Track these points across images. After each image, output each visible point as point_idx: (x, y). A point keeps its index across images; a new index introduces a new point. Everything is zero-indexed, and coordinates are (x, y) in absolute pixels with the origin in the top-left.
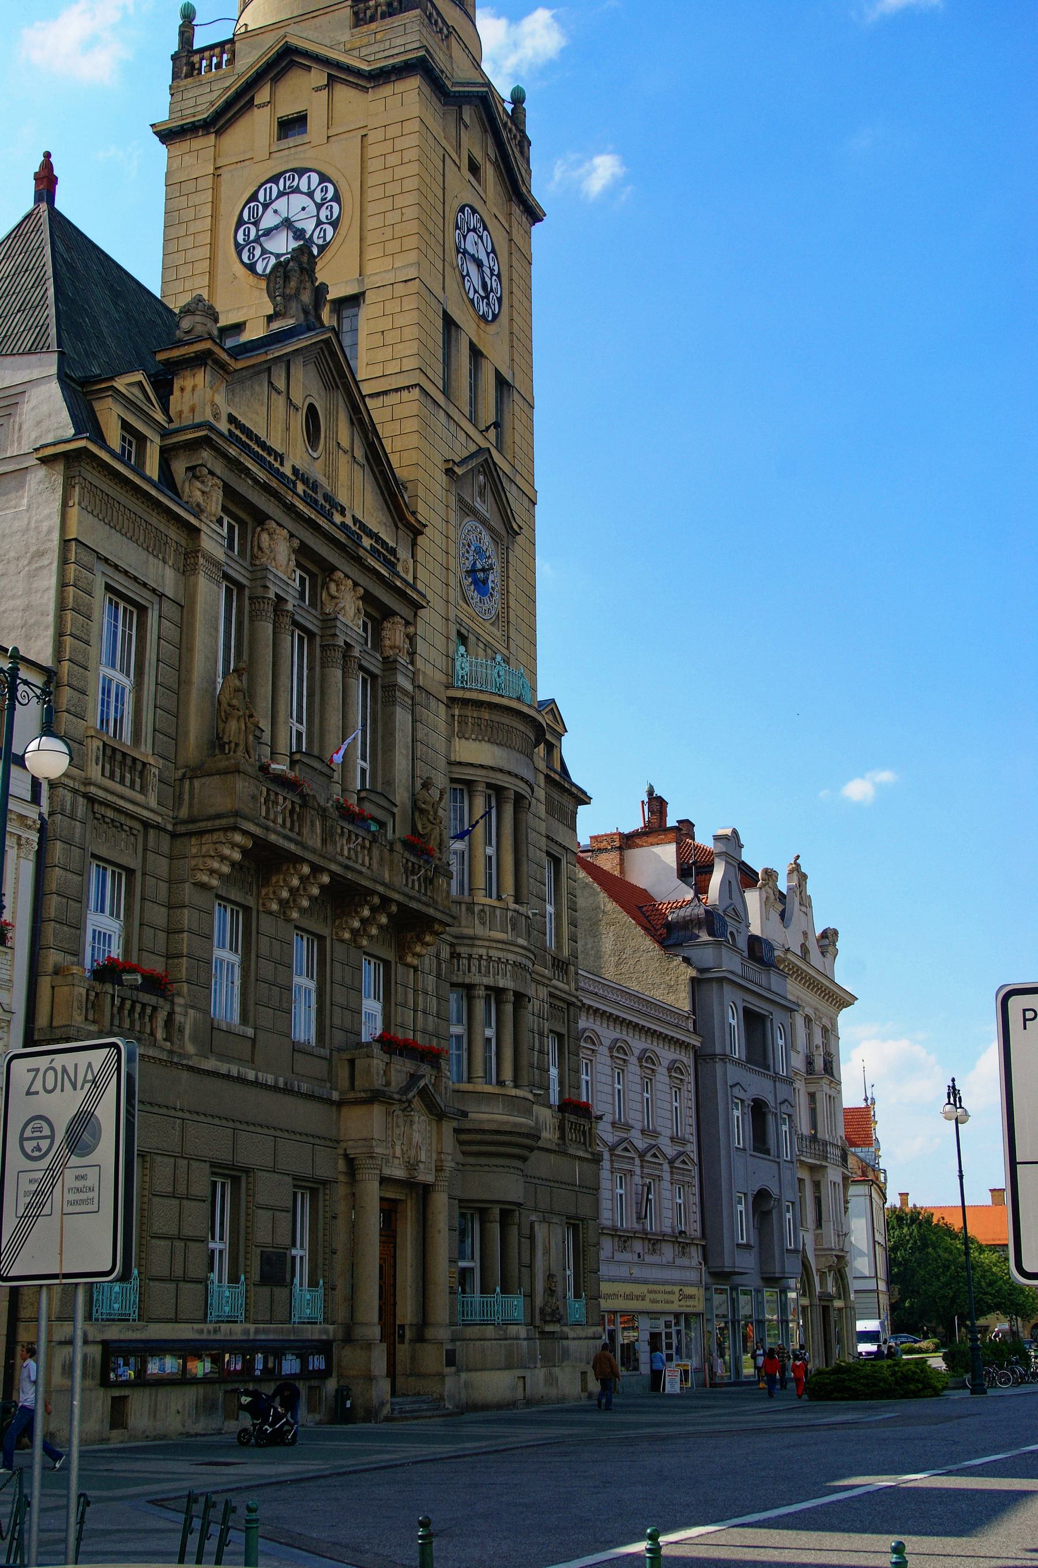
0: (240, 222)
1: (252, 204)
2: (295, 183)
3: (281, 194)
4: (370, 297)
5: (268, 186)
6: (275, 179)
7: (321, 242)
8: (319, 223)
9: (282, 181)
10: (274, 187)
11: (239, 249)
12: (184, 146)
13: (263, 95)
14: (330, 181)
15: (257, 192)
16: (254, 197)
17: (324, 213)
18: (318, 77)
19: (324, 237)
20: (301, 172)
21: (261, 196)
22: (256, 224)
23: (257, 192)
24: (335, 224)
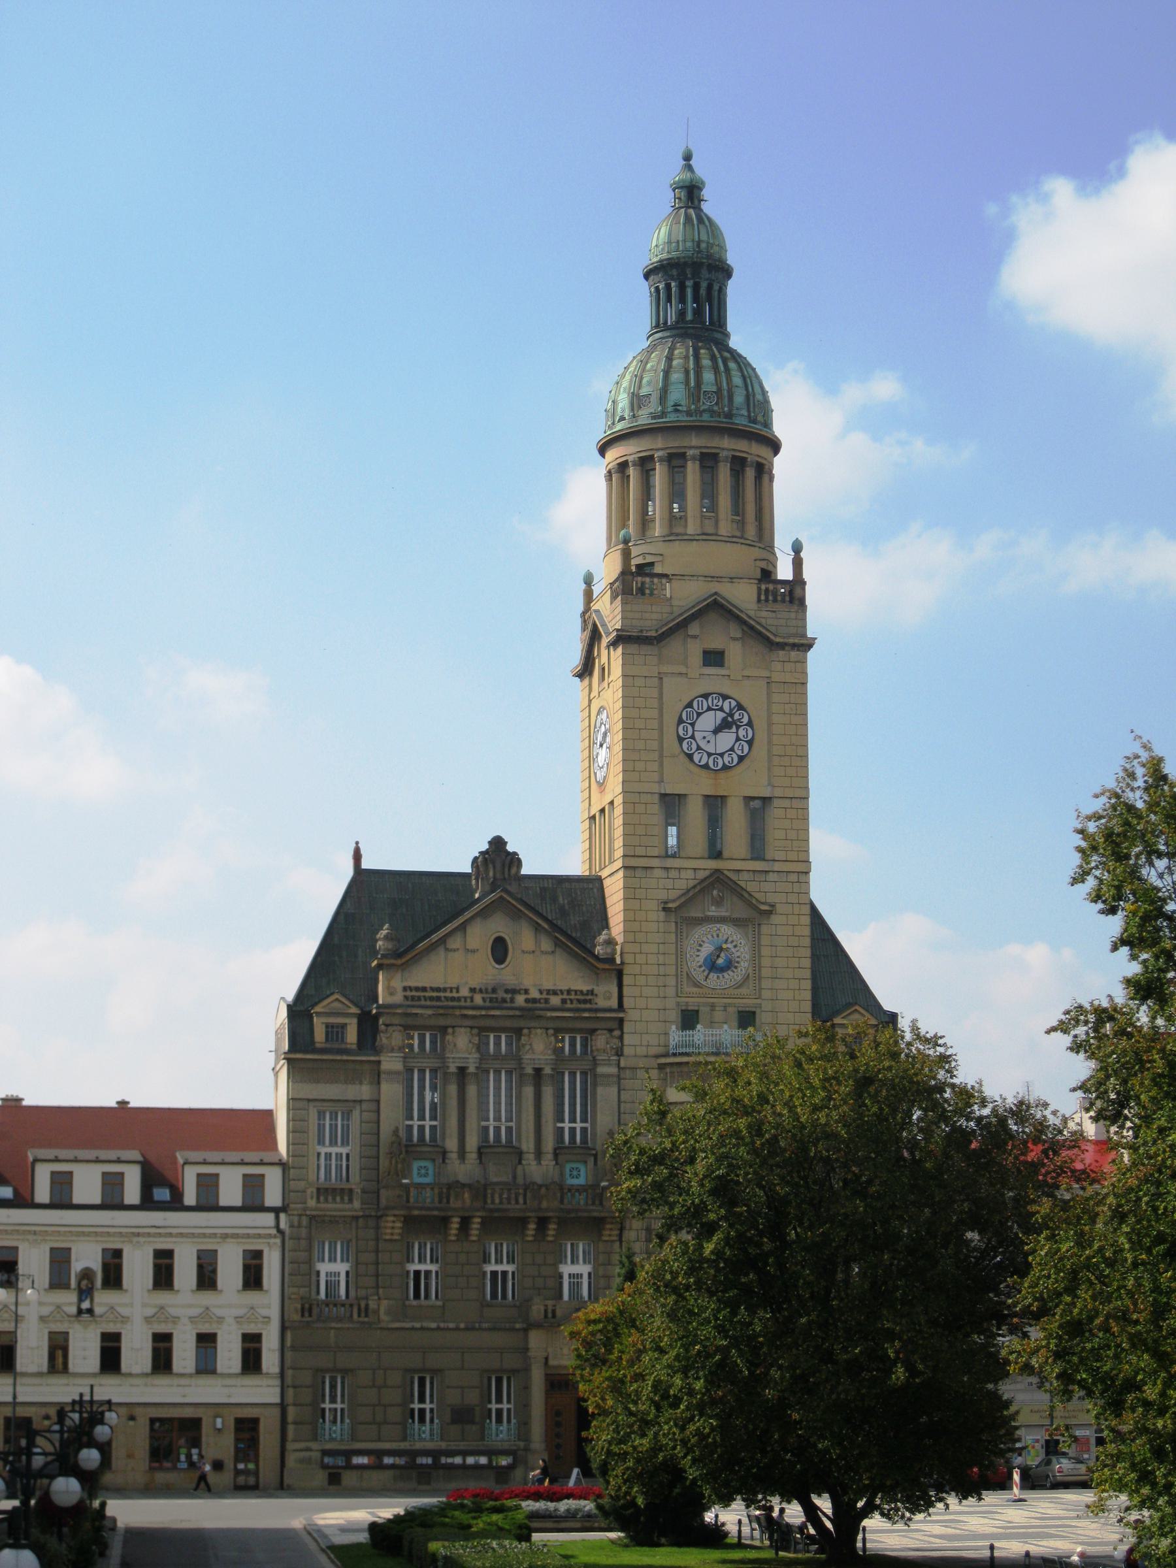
0: (681, 721)
1: (689, 709)
2: (720, 704)
3: (709, 709)
4: (776, 803)
5: (700, 699)
6: (706, 696)
7: (740, 753)
8: (738, 739)
9: (710, 699)
10: (704, 701)
11: (681, 740)
12: (633, 648)
13: (694, 629)
14: (745, 710)
15: (693, 700)
16: (690, 705)
17: (742, 732)
18: (735, 630)
19: (742, 750)
20: (725, 697)
21: (695, 704)
22: (693, 725)
23: (693, 700)
24: (750, 743)
